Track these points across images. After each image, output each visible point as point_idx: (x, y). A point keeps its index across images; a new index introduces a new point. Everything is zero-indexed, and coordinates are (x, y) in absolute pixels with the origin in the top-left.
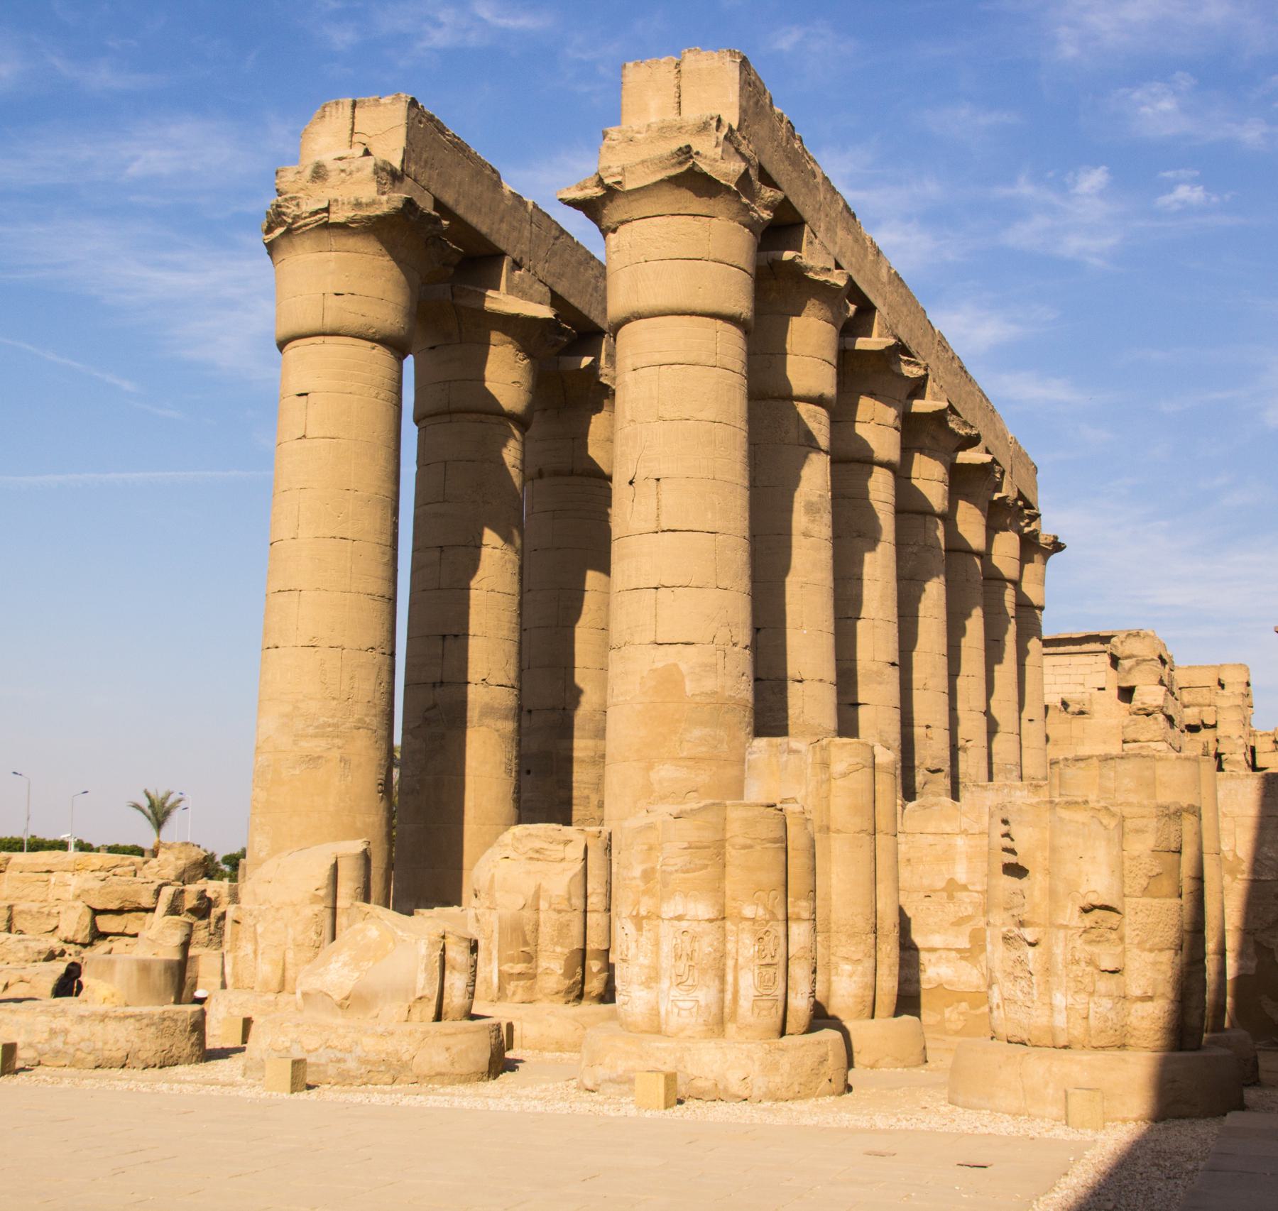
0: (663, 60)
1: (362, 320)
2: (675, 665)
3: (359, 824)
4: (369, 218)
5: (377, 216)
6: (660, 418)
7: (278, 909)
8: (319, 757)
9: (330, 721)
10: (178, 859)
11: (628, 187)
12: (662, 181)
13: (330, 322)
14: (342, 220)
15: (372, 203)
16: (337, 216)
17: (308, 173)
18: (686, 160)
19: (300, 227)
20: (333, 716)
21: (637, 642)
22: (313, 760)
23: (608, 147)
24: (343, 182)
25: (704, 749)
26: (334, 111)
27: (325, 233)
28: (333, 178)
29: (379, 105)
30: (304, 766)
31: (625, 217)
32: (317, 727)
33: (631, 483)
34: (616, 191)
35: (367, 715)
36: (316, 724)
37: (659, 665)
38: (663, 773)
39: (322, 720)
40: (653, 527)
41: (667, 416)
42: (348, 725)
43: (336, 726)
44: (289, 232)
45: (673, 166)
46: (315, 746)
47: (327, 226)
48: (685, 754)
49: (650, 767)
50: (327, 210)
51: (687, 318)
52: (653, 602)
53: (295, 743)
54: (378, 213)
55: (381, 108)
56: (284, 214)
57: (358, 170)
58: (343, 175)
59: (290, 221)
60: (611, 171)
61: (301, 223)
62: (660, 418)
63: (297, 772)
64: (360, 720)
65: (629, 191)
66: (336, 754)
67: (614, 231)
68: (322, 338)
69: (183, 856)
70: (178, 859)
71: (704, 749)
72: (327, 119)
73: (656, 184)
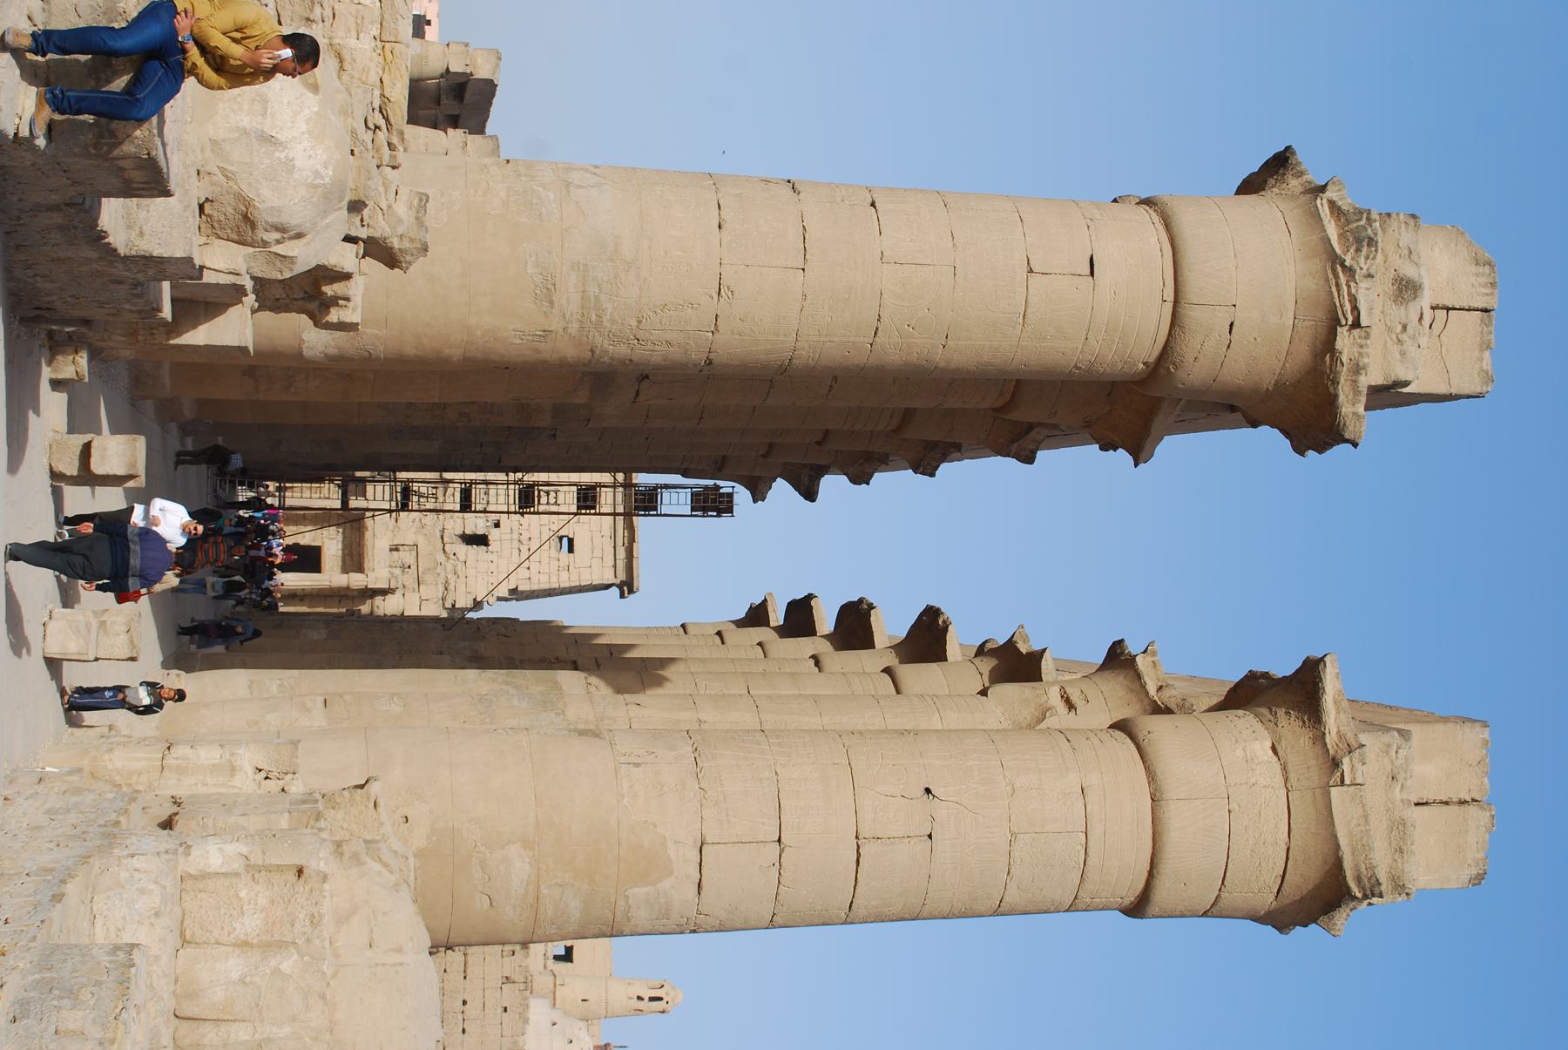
0: (1486, 780)
1: (1189, 358)
2: (671, 873)
4: (1335, 382)
5: (1336, 396)
7: (323, 997)
8: (551, 303)
9: (606, 318)
10: (401, 237)
11: (1335, 792)
12: (1338, 847)
13: (1194, 315)
14: (1339, 344)
15: (1356, 392)
16: (1345, 341)
17: (1409, 271)
18: (1362, 888)
20: (613, 321)
22: (548, 296)
23: (1389, 746)
24: (1389, 329)
26: (1484, 280)
27: (1322, 315)
28: (1397, 314)
29: (1482, 351)
31: (1292, 777)
32: (597, 298)
33: (928, 791)
36: (603, 297)
37: (672, 851)
44: (1335, 260)
45: (1356, 867)
47: (1334, 323)
50: (1356, 324)
51: (1147, 866)
54: (1342, 397)
55: (1477, 354)
56: (1358, 250)
57: (1403, 354)
58: (1399, 328)
60: (1358, 766)
61: (1343, 279)
68: (1170, 297)
69: (406, 244)
71: (550, 913)
72: (1474, 269)
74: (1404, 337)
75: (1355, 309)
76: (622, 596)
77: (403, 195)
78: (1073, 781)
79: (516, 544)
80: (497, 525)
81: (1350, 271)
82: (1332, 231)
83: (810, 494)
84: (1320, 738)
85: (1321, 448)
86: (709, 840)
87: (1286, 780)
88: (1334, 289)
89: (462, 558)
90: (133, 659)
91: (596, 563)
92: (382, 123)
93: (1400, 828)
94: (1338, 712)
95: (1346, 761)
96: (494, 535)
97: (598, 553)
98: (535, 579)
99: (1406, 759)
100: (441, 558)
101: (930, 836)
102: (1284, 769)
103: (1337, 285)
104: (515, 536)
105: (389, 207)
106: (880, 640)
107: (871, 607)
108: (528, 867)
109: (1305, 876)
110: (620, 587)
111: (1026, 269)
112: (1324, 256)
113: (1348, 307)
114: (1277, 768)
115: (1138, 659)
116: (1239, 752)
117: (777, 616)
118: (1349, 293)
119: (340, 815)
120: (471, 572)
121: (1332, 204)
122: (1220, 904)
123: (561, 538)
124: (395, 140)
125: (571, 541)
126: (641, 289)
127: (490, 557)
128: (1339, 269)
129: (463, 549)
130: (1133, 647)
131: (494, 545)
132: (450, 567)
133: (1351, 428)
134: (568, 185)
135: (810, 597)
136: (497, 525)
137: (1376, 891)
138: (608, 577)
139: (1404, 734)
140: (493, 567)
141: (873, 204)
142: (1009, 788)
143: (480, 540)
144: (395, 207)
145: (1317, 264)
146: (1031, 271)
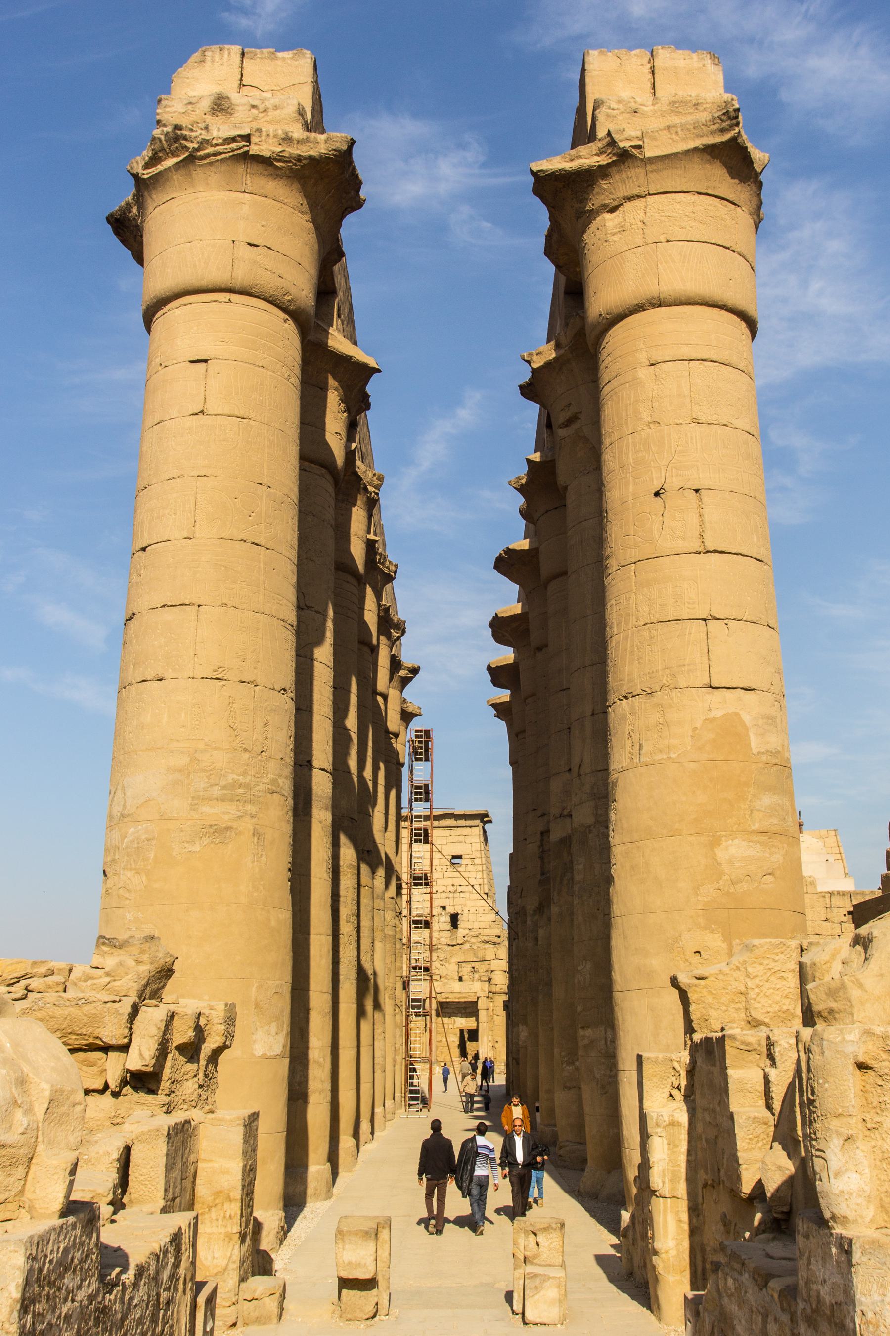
0: (634, 53)
1: (279, 282)
2: (737, 714)
3: (273, 923)
4: (299, 159)
5: (311, 158)
6: (696, 421)
8: (228, 828)
10: (139, 962)
11: (648, 154)
12: (696, 150)
13: (241, 276)
14: (266, 154)
15: (307, 140)
16: (263, 147)
17: (206, 104)
18: (731, 127)
19: (208, 156)
20: (245, 774)
21: (682, 684)
22: (219, 832)
23: (608, 116)
25: (775, 821)
26: (217, 57)
27: (241, 169)
29: (276, 58)
30: (206, 841)
31: (636, 191)
32: (224, 788)
33: (657, 494)
34: (633, 157)
35: (280, 776)
36: (223, 783)
37: (717, 713)
38: (733, 850)
39: (231, 777)
40: (696, 546)
41: (702, 419)
42: (262, 787)
43: (248, 786)
45: (712, 133)
46: (221, 812)
47: (246, 157)
48: (756, 826)
49: (714, 843)
50: (247, 138)
52: (703, 636)
53: (193, 808)
54: (312, 153)
55: (279, 63)
56: (185, 138)
57: (276, 108)
58: (254, 111)
59: (191, 146)
61: (210, 150)
62: (696, 421)
63: (197, 848)
64: (274, 781)
65: (650, 159)
66: (247, 825)
67: (613, 210)
70: (139, 962)
71: (775, 821)
73: (687, 153)
74: (261, 108)
75: (233, 139)
76: (490, 822)
77: (96, 961)
78: (644, 373)
79: (457, 895)
80: (444, 908)
82: (170, 162)
84: (603, 171)
85: (356, 183)
86: (707, 681)
87: (639, 197)
88: (219, 158)
89: (467, 931)
90: (563, 1225)
91: (468, 840)
92: (23, 983)
93: (676, 106)
94: (580, 157)
95: (621, 145)
96: (450, 910)
97: (462, 839)
98: (481, 881)
99: (619, 102)
100: (467, 946)
101: (697, 491)
102: (630, 199)
103: (215, 155)
104: (451, 895)
105: (108, 974)
108: (736, 841)
109: (718, 178)
110: (485, 823)
111: (201, 415)
112: (191, 167)
113: (234, 146)
114: (628, 206)
115: (535, 366)
116: (615, 238)
118: (221, 145)
119: (713, 1013)
120: (476, 925)
121: (147, 166)
122: (745, 253)
124: (43, 970)
125: (454, 857)
126: (215, 749)
127: (466, 912)
128: (202, 153)
129: (461, 931)
131: (458, 910)
132: (473, 940)
133: (338, 145)
134: (123, 816)
136: (444, 908)
137: (732, 114)
138: (477, 831)
139: (597, 105)
140: (473, 910)
141: (144, 549)
142: (652, 426)
143: (454, 920)
144: (107, 969)
145: (198, 173)
146: (202, 412)
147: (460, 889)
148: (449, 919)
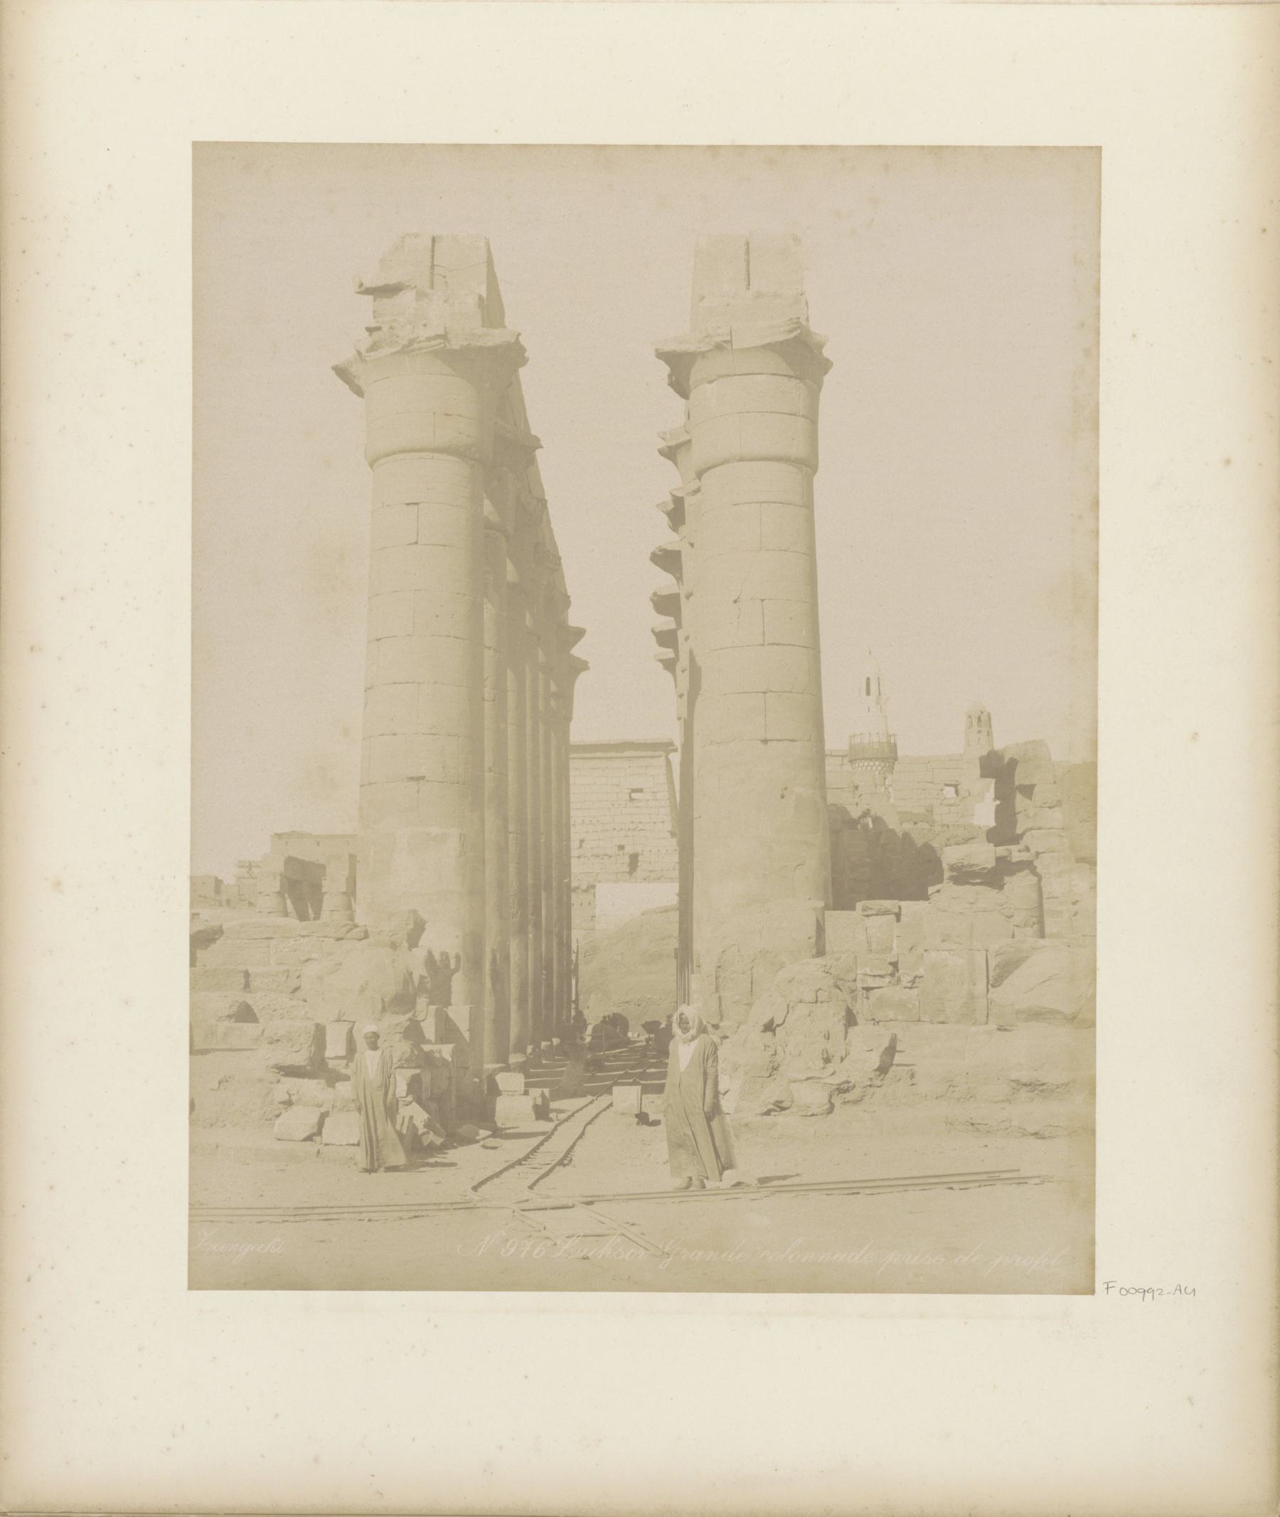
18: (795, 329)
33: (735, 602)
50: (444, 337)
67: (710, 382)
73: (764, 347)
80: (621, 847)
81: (411, 342)
83: (580, 633)
84: (703, 355)
85: (523, 350)
96: (629, 849)
102: (721, 376)
106: (675, 590)
107: (655, 594)
113: (433, 343)
117: (668, 653)
123: (631, 799)
125: (634, 791)
130: (662, 444)
135: (653, 631)
136: (621, 847)
138: (662, 761)
147: (641, 826)
148: (627, 860)
